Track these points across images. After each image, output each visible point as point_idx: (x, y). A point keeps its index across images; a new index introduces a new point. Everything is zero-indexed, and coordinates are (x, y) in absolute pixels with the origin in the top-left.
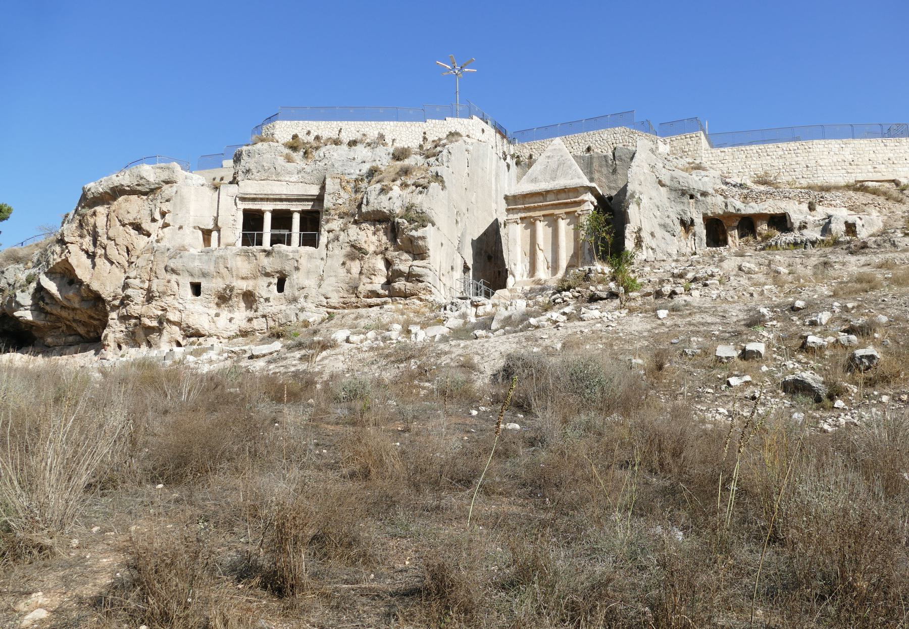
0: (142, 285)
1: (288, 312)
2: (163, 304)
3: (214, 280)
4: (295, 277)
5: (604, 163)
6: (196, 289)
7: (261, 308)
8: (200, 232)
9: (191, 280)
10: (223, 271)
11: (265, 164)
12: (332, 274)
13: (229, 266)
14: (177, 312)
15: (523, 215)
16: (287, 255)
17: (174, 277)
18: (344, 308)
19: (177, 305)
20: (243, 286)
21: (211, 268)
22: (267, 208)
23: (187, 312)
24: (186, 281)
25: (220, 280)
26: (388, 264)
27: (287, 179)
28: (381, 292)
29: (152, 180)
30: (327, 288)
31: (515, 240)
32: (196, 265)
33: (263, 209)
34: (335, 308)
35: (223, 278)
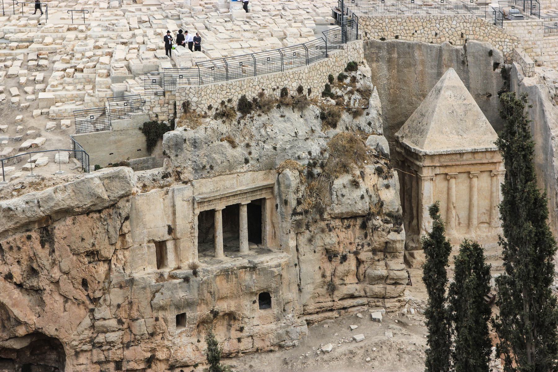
0: (121, 327)
1: (280, 331)
2: (153, 346)
3: (198, 308)
4: (281, 294)
5: (454, 57)
6: (180, 320)
7: (246, 329)
8: (154, 244)
9: (176, 313)
10: (207, 296)
11: (214, 155)
12: (309, 281)
13: (212, 290)
14: (165, 350)
15: (438, 171)
16: (272, 272)
17: (161, 314)
18: (317, 313)
19: (166, 343)
20: (223, 306)
21: (193, 295)
22: (220, 206)
23: (175, 348)
24: (171, 316)
25: (203, 306)
26: (359, 262)
27: (238, 171)
28: (356, 294)
29: (106, 197)
30: (306, 297)
31: (430, 197)
32: (181, 294)
33: (217, 208)
34: (311, 314)
35: (207, 304)
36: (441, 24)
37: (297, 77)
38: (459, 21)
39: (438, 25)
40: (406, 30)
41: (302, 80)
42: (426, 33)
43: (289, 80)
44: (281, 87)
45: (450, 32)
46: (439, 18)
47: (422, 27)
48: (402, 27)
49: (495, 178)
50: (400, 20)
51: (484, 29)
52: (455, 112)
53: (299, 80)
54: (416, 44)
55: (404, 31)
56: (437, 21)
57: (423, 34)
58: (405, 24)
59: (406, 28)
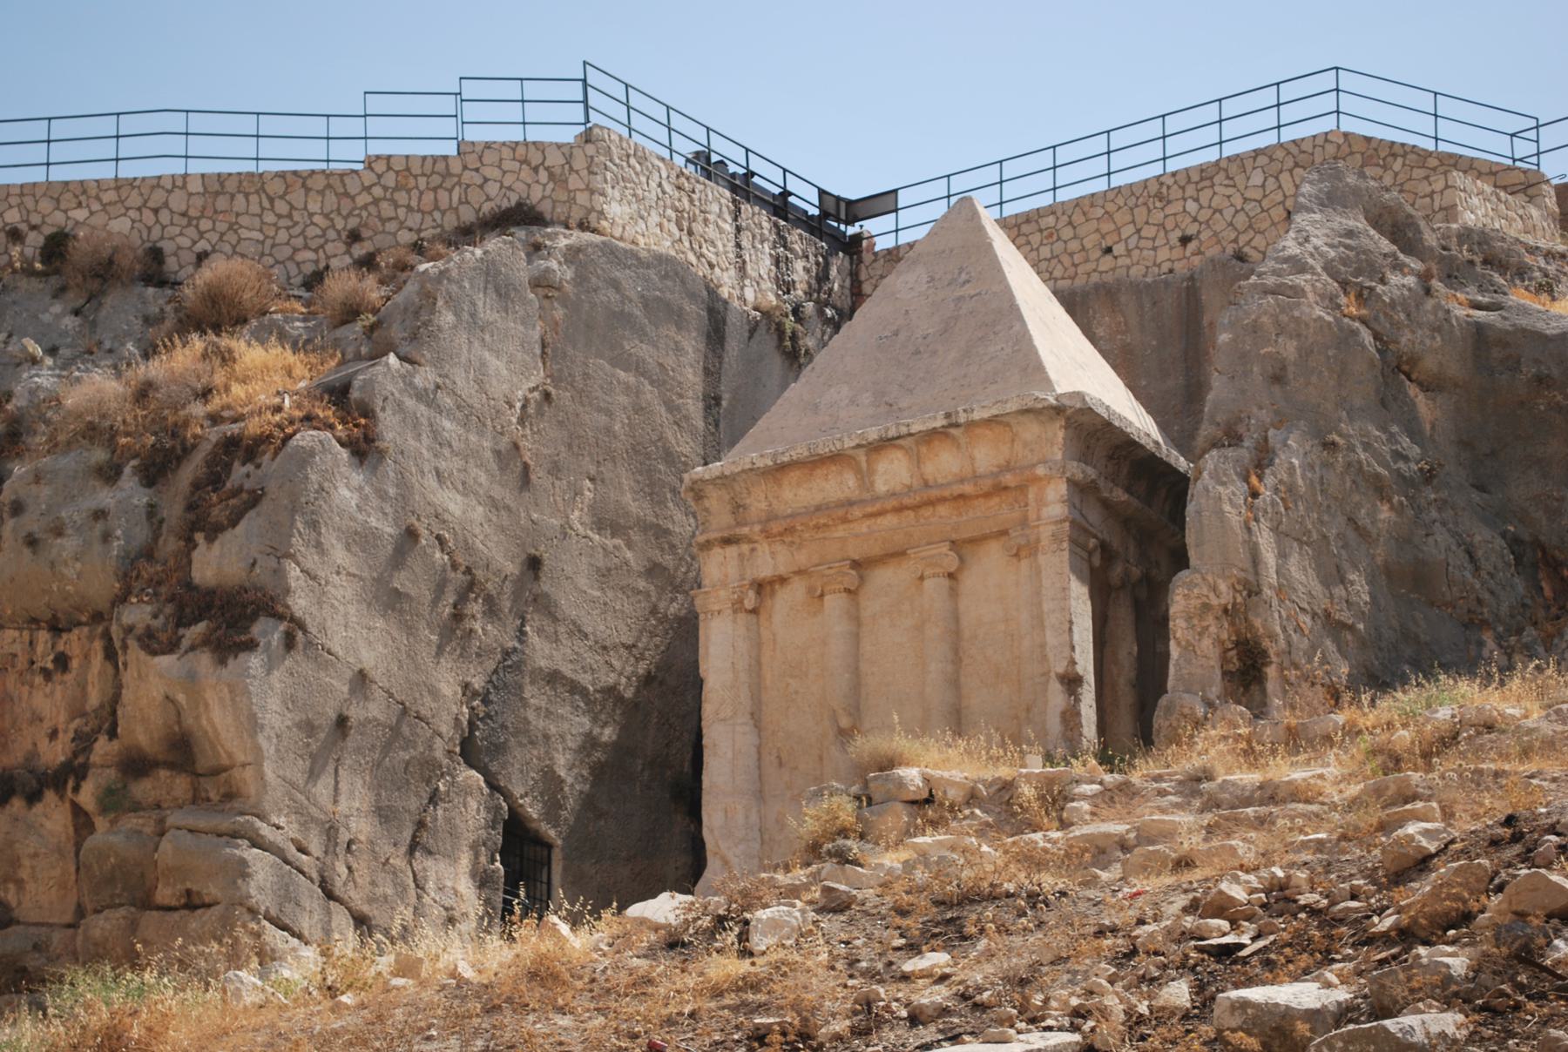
36: (1205, 196)
37: (135, 199)
38: (1276, 166)
39: (1191, 206)
40: (1071, 255)
41: (164, 217)
42: (1150, 244)
43: (96, 206)
44: (48, 231)
45: (1241, 218)
46: (1195, 178)
47: (1128, 231)
48: (1059, 247)
49: (1025, 563)
50: (1051, 220)
51: (1379, 171)
52: (902, 336)
53: (149, 217)
54: (1097, 287)
55: (1066, 260)
56: (1190, 191)
57: (1136, 253)
58: (1067, 233)
59: (1074, 246)
